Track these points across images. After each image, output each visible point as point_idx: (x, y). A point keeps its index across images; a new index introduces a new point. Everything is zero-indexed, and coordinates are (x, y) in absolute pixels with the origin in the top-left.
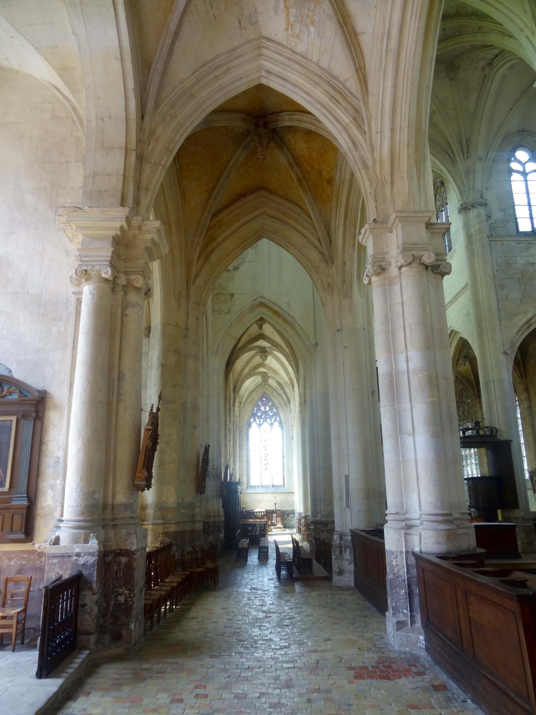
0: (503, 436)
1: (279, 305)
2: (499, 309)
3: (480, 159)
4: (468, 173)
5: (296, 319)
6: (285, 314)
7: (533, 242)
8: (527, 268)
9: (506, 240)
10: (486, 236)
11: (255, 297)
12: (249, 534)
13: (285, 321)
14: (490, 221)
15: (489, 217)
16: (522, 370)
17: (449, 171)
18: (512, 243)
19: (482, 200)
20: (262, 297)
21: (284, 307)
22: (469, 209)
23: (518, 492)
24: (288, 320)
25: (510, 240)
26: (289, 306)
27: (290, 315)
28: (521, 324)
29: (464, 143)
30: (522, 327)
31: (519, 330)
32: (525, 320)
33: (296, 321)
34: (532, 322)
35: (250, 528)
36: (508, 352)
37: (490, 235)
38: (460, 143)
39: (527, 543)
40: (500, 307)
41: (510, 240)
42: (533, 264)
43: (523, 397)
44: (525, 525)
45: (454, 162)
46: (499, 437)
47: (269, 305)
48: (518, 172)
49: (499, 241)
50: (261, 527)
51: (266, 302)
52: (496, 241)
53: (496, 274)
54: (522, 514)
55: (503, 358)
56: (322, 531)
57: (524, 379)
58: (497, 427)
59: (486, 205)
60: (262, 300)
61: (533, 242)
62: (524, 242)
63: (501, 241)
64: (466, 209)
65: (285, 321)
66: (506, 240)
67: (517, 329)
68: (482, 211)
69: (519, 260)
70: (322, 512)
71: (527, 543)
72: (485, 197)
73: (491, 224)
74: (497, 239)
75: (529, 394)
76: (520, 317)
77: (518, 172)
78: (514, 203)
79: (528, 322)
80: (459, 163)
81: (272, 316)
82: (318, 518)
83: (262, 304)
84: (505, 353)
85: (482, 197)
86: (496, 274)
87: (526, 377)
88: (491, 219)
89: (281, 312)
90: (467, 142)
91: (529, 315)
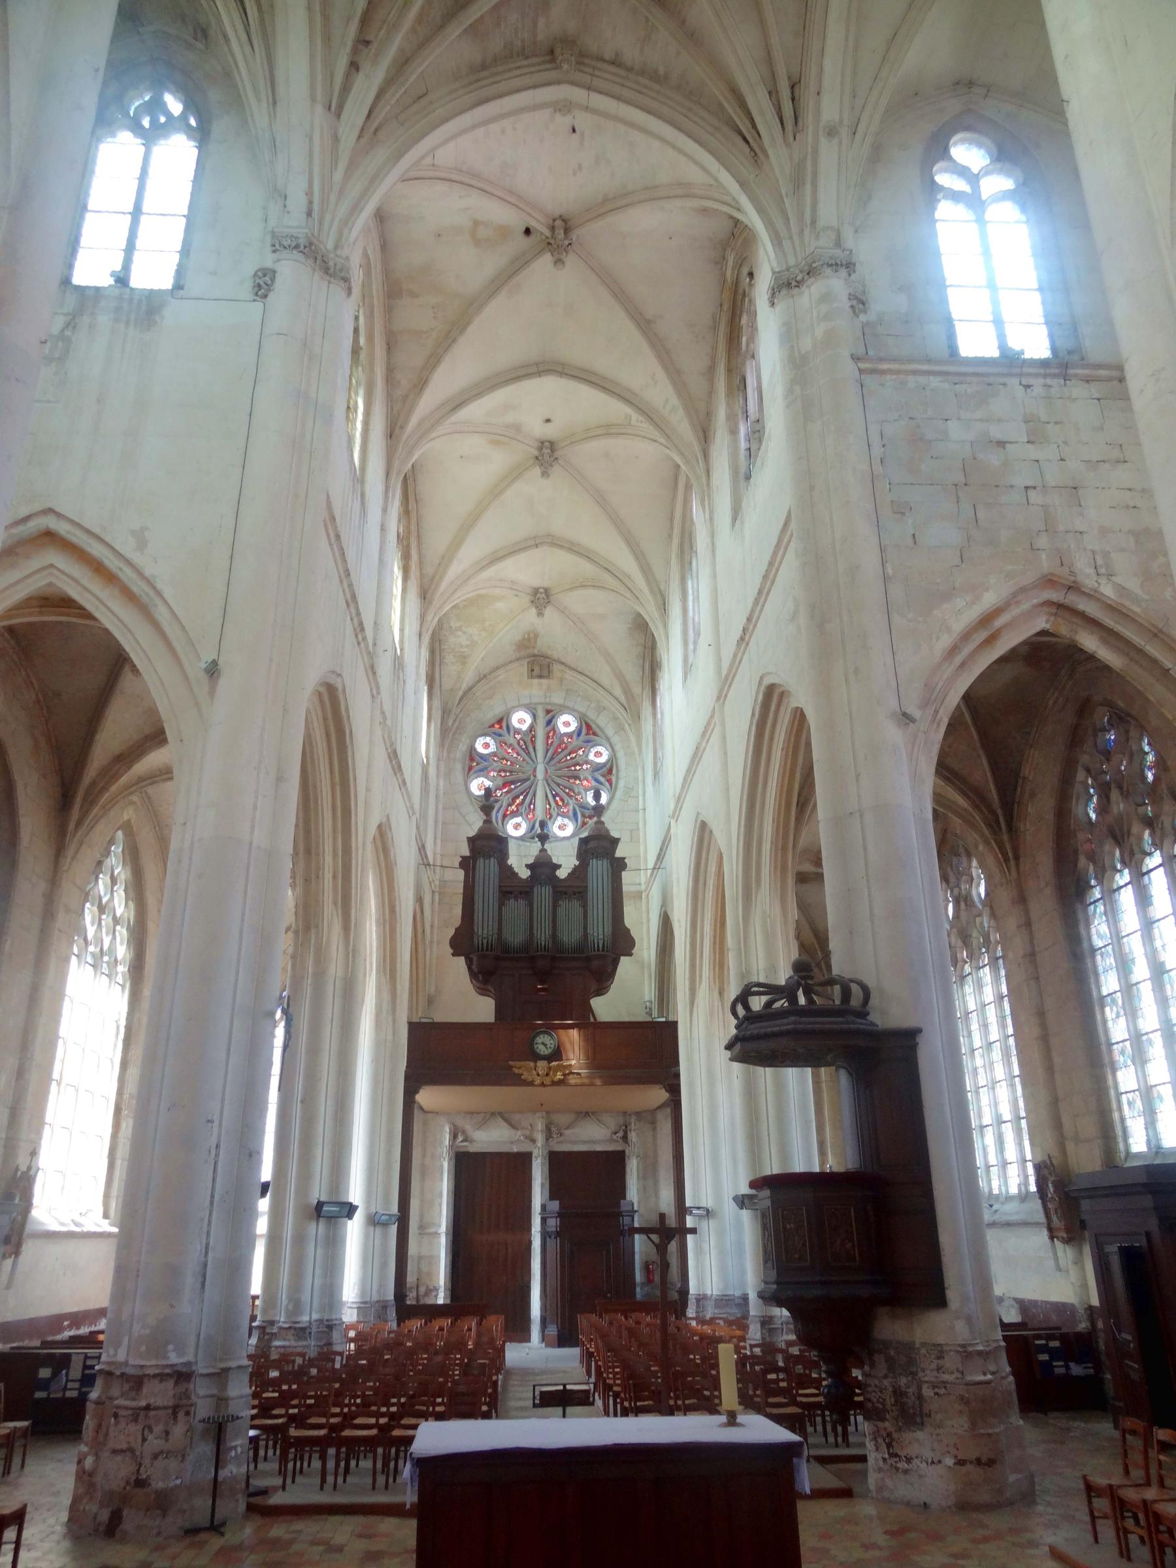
0: (889, 1014)
1: (108, 539)
2: (886, 579)
3: (832, 132)
4: (797, 183)
5: (159, 586)
6: (127, 570)
7: (1002, 380)
8: (981, 456)
9: (915, 372)
10: (845, 353)
11: (24, 512)
12: (40, 1395)
13: (130, 596)
14: (863, 318)
15: (859, 302)
16: (1005, 837)
17: (743, 184)
18: (934, 382)
19: (838, 252)
20: (50, 511)
21: (127, 546)
22: (799, 284)
23: (944, 1239)
24: (135, 589)
25: (929, 373)
26: (142, 544)
27: (140, 574)
28: (959, 625)
29: (785, 94)
30: (966, 636)
31: (954, 650)
32: (973, 614)
33: (159, 594)
34: (999, 622)
35: (45, 1373)
36: (917, 713)
37: (862, 351)
38: (773, 93)
39: (979, 1462)
40: (890, 571)
41: (929, 373)
42: (1001, 444)
43: (1012, 923)
44: (969, 1378)
45: (756, 155)
46: (874, 1017)
47: (74, 540)
48: (956, 196)
49: (890, 371)
50: (85, 1367)
51: (62, 528)
52: (883, 372)
53: (878, 469)
54: (962, 1333)
55: (894, 734)
56: (116, 1416)
57: (1012, 863)
58: (871, 983)
59: (850, 266)
60: (52, 523)
61: (1002, 380)
62: (974, 379)
63: (898, 372)
64: (789, 285)
65: (130, 596)
66: (915, 372)
67: (946, 641)
68: (836, 284)
69: (955, 430)
70: (136, 1328)
71: (979, 1462)
72: (849, 242)
73: (864, 326)
74: (885, 366)
75: (1027, 912)
76: (959, 603)
77: (956, 196)
78: (944, 279)
79: (986, 620)
80: (770, 152)
81: (85, 582)
82: (121, 1356)
83: (49, 537)
84: (906, 718)
85: (838, 243)
86: (878, 469)
87: (1017, 858)
88: (865, 312)
89: (111, 563)
90: (792, 87)
91: (989, 600)
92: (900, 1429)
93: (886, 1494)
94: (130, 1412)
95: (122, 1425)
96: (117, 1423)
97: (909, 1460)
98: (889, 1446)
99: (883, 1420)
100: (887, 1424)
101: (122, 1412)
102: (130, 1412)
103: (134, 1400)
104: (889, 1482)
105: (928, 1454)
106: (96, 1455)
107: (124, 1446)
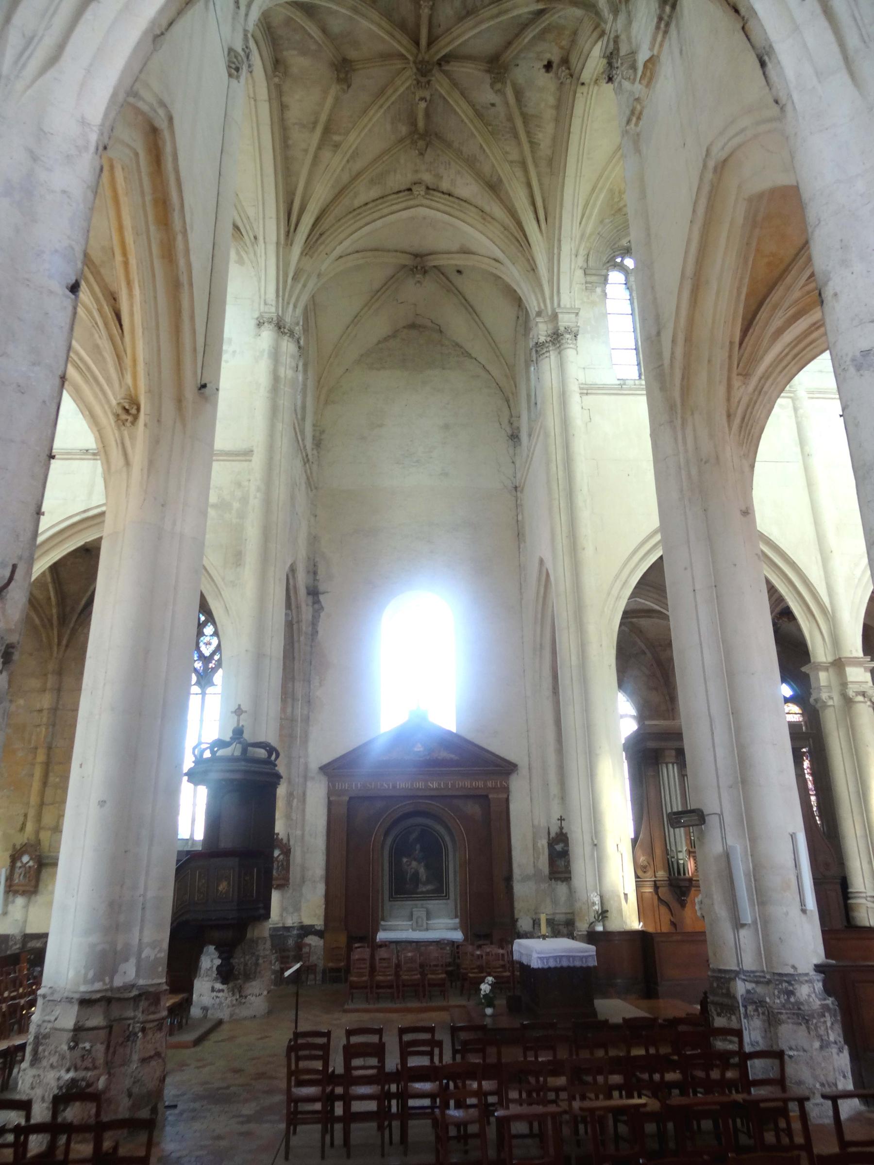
70: (146, 952)
92: (244, 983)
93: (235, 1017)
94: (155, 1023)
95: (150, 1035)
96: (144, 1036)
97: (246, 997)
98: (240, 992)
99: (237, 979)
100: (239, 981)
101: (148, 1026)
102: (155, 1023)
103: (154, 1013)
104: (237, 1011)
105: (257, 991)
106: (109, 1074)
107: (152, 1053)
